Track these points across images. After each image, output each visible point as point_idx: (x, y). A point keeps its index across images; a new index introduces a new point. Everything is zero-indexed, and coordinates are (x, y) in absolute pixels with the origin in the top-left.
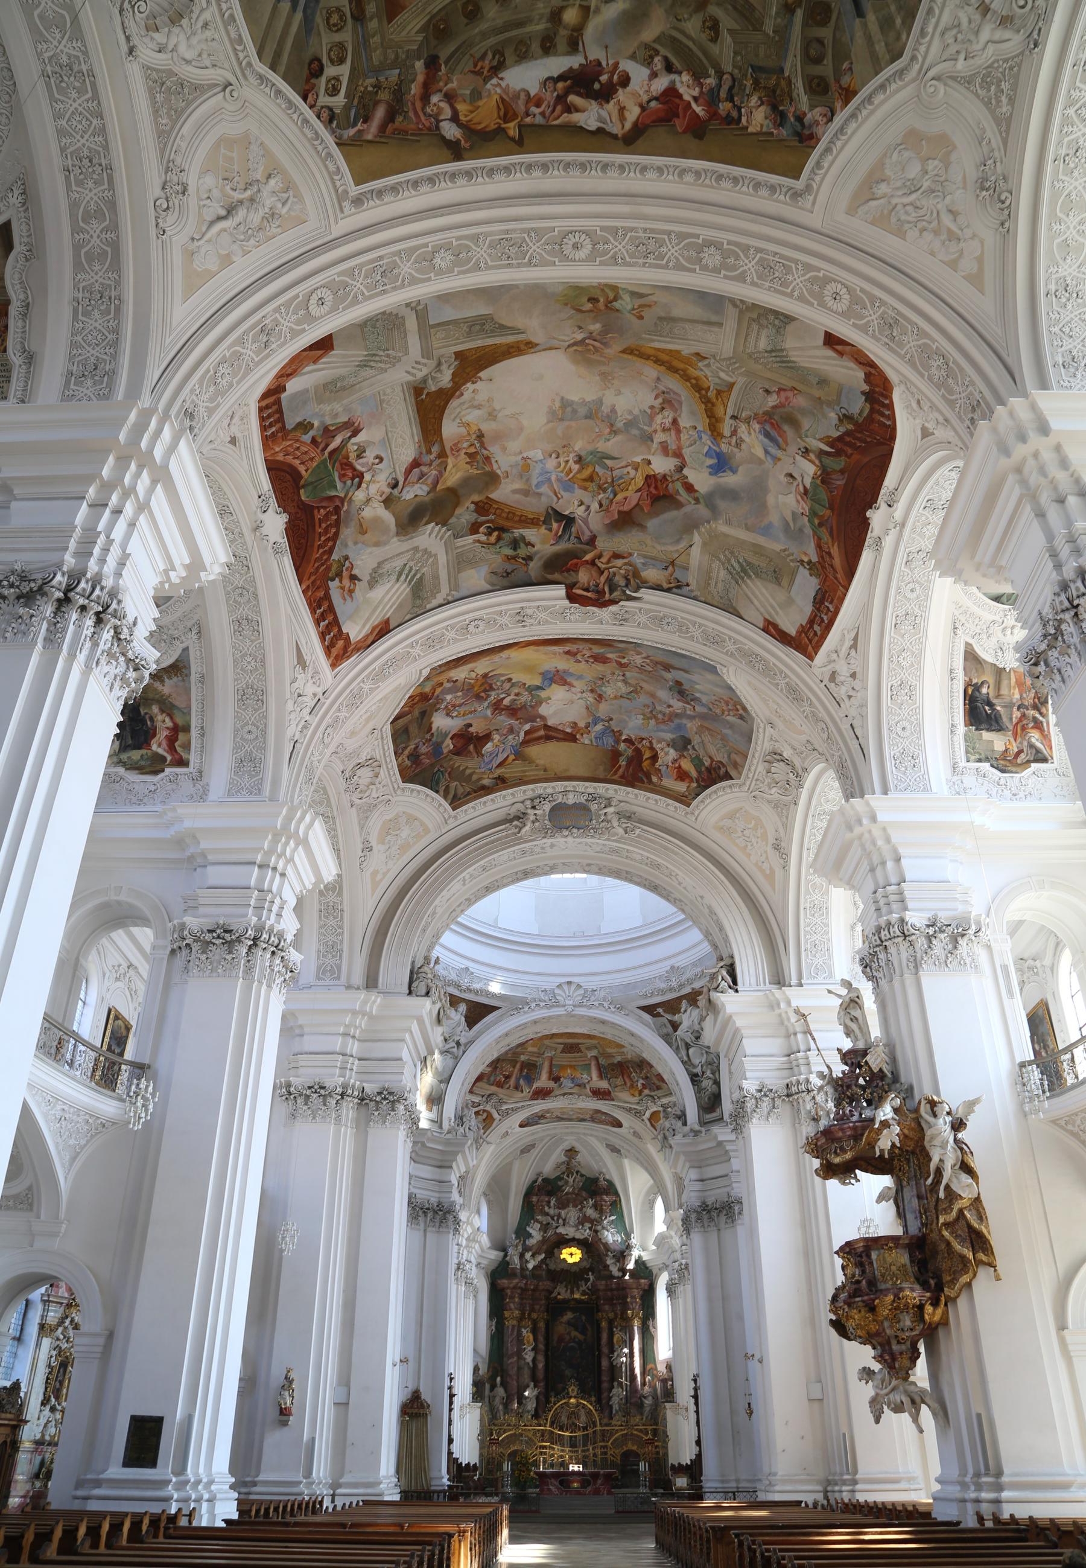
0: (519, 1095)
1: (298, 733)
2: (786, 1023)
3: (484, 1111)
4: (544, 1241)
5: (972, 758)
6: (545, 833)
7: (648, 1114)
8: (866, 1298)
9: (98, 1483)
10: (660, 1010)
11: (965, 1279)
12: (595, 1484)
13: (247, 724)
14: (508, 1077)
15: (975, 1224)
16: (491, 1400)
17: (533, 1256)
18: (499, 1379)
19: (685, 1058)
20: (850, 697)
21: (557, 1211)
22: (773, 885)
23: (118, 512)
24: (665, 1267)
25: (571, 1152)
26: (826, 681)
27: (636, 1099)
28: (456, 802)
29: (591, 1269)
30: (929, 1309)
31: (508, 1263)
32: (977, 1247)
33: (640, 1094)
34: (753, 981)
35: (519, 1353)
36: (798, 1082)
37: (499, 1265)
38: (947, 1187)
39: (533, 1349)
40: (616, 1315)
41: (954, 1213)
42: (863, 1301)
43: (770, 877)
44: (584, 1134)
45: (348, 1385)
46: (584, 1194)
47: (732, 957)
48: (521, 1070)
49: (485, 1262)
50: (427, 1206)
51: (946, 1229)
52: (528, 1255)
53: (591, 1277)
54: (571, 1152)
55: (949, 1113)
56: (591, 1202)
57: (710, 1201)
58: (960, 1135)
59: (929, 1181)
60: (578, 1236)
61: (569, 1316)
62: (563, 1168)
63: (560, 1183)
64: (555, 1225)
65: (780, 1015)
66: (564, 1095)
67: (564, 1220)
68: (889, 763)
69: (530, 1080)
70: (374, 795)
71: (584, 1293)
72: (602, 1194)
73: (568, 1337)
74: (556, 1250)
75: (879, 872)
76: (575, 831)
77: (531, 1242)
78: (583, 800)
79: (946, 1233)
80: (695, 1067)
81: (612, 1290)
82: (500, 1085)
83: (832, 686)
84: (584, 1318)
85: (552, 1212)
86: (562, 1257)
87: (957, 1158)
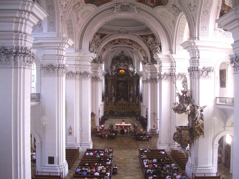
1: (62, 14)
5: (219, 27)
6: (119, 12)
7: (140, 49)
9: (45, 166)
10: (144, 37)
13: (50, 14)
16: (106, 99)
17: (114, 72)
18: (107, 96)
19: (149, 47)
20: (194, 11)
22: (171, 29)
23: (22, 23)
25: (123, 52)
26: (188, 5)
27: (137, 46)
28: (98, 6)
29: (126, 75)
31: (109, 74)
34: (165, 50)
35: (111, 91)
36: (173, 73)
43: (171, 27)
45: (82, 128)
46: (125, 60)
47: (161, 43)
52: (113, 72)
53: (126, 77)
57: (152, 78)
60: (123, 68)
61: (121, 83)
62: (121, 54)
63: (120, 57)
68: (200, 28)
70: (79, 8)
73: (121, 88)
75: (194, 54)
76: (126, 12)
77: (113, 69)
78: (128, 4)
80: (151, 49)
83: (190, 6)
85: (118, 63)
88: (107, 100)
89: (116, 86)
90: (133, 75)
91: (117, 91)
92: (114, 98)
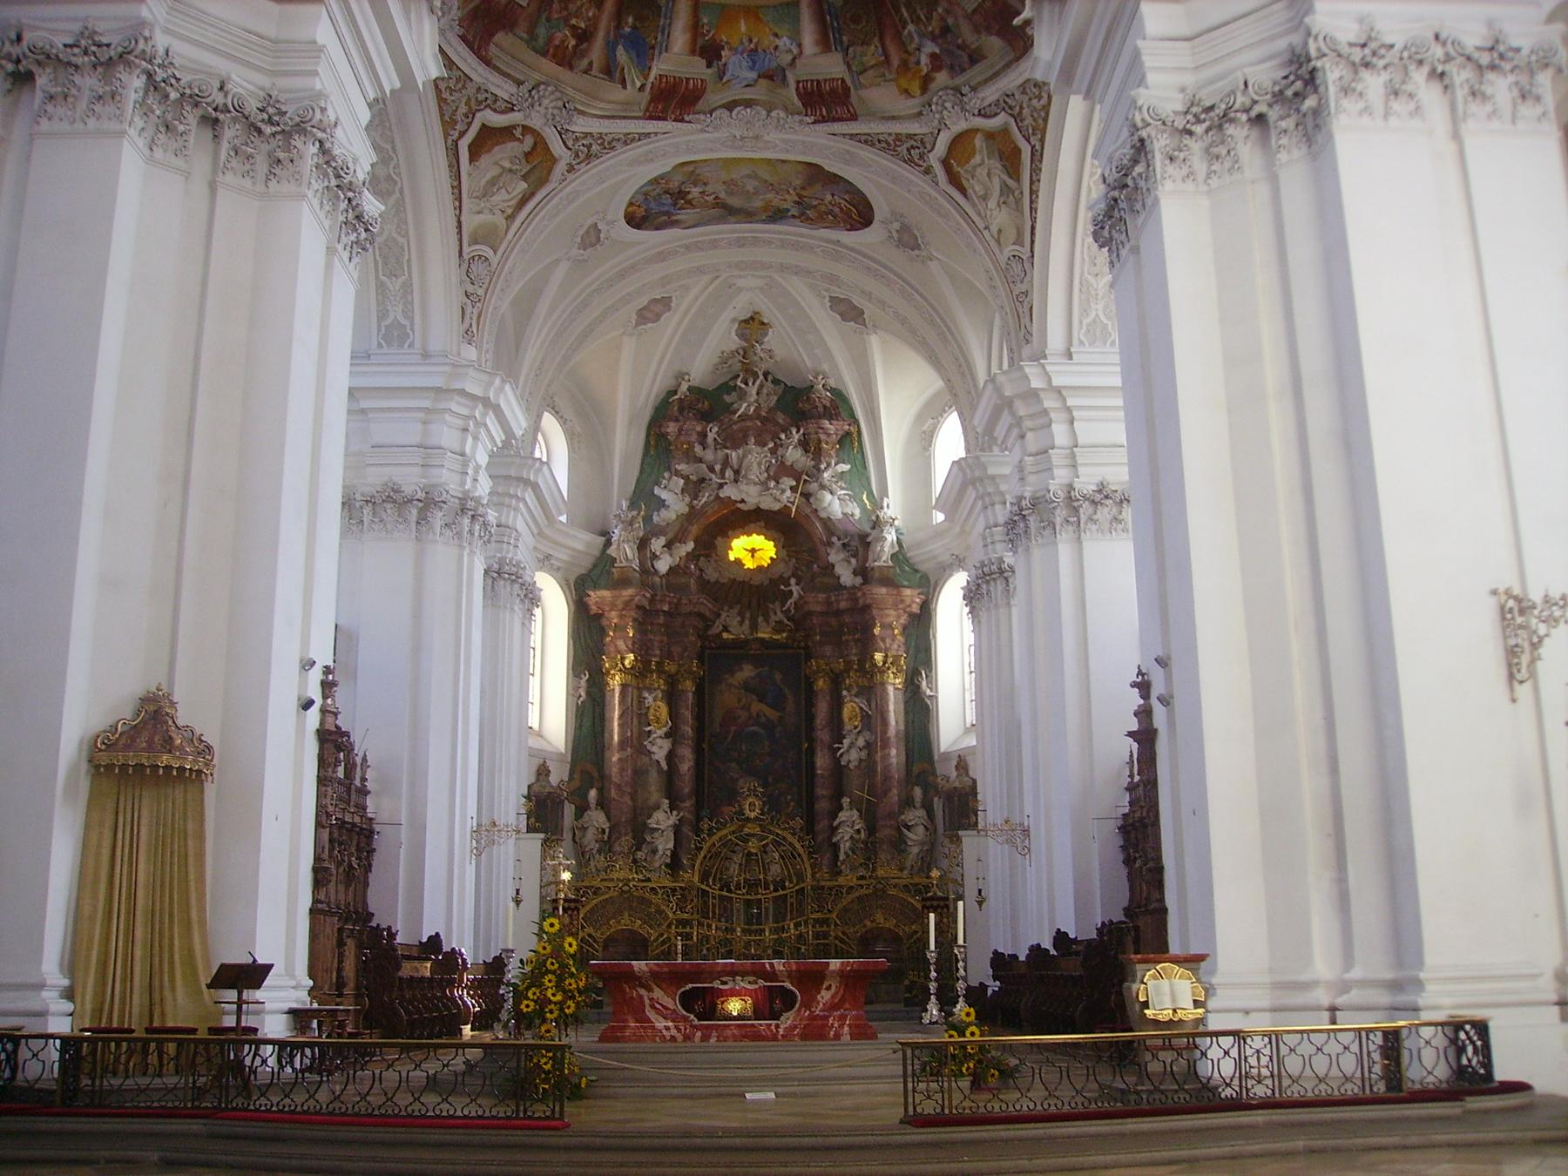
0: (616, 93)
3: (526, 129)
4: (692, 515)
12: (807, 1004)
14: (584, 37)
17: (668, 546)
18: (593, 793)
21: (720, 454)
24: (959, 563)
25: (753, 325)
27: (912, 105)
31: (614, 560)
33: (924, 89)
37: (595, 566)
39: (667, 735)
40: (848, 663)
44: (783, 268)
46: (781, 418)
48: (618, 17)
49: (562, 555)
50: (219, 99)
52: (657, 544)
53: (795, 589)
54: (753, 325)
56: (796, 437)
60: (768, 504)
61: (747, 672)
63: (727, 399)
64: (716, 479)
66: (730, 106)
67: (737, 472)
69: (644, 52)
71: (779, 627)
72: (820, 417)
73: (744, 715)
74: (719, 541)
81: (839, 613)
82: (565, 59)
84: (778, 676)
85: (709, 455)
86: (732, 556)
88: (591, 835)
89: (689, 686)
90: (863, 572)
91: (698, 751)
92: (663, 820)
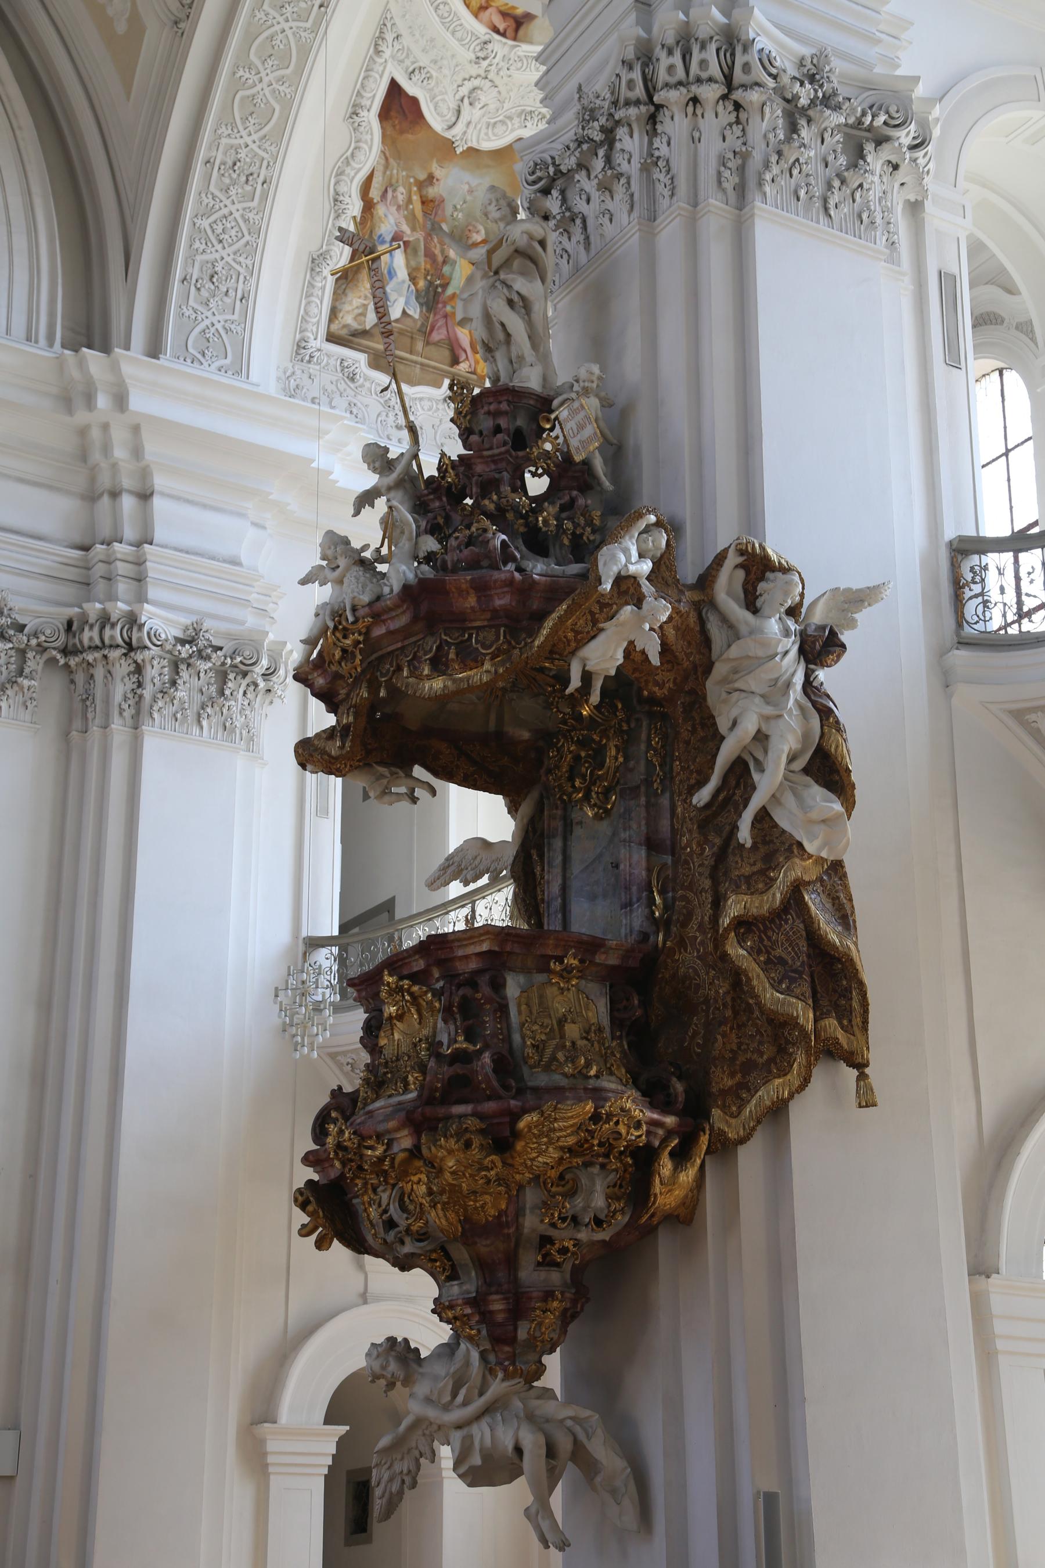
2: (96, 456)
8: (490, 1106)
11: (768, 1093)
15: (831, 931)
30: (666, 1166)
32: (825, 1002)
36: (105, 620)
38: (763, 816)
41: (777, 896)
42: (480, 1116)
51: (741, 942)
55: (793, 612)
58: (822, 675)
59: (703, 796)
65: (83, 432)
79: (737, 952)
87: (806, 736)
